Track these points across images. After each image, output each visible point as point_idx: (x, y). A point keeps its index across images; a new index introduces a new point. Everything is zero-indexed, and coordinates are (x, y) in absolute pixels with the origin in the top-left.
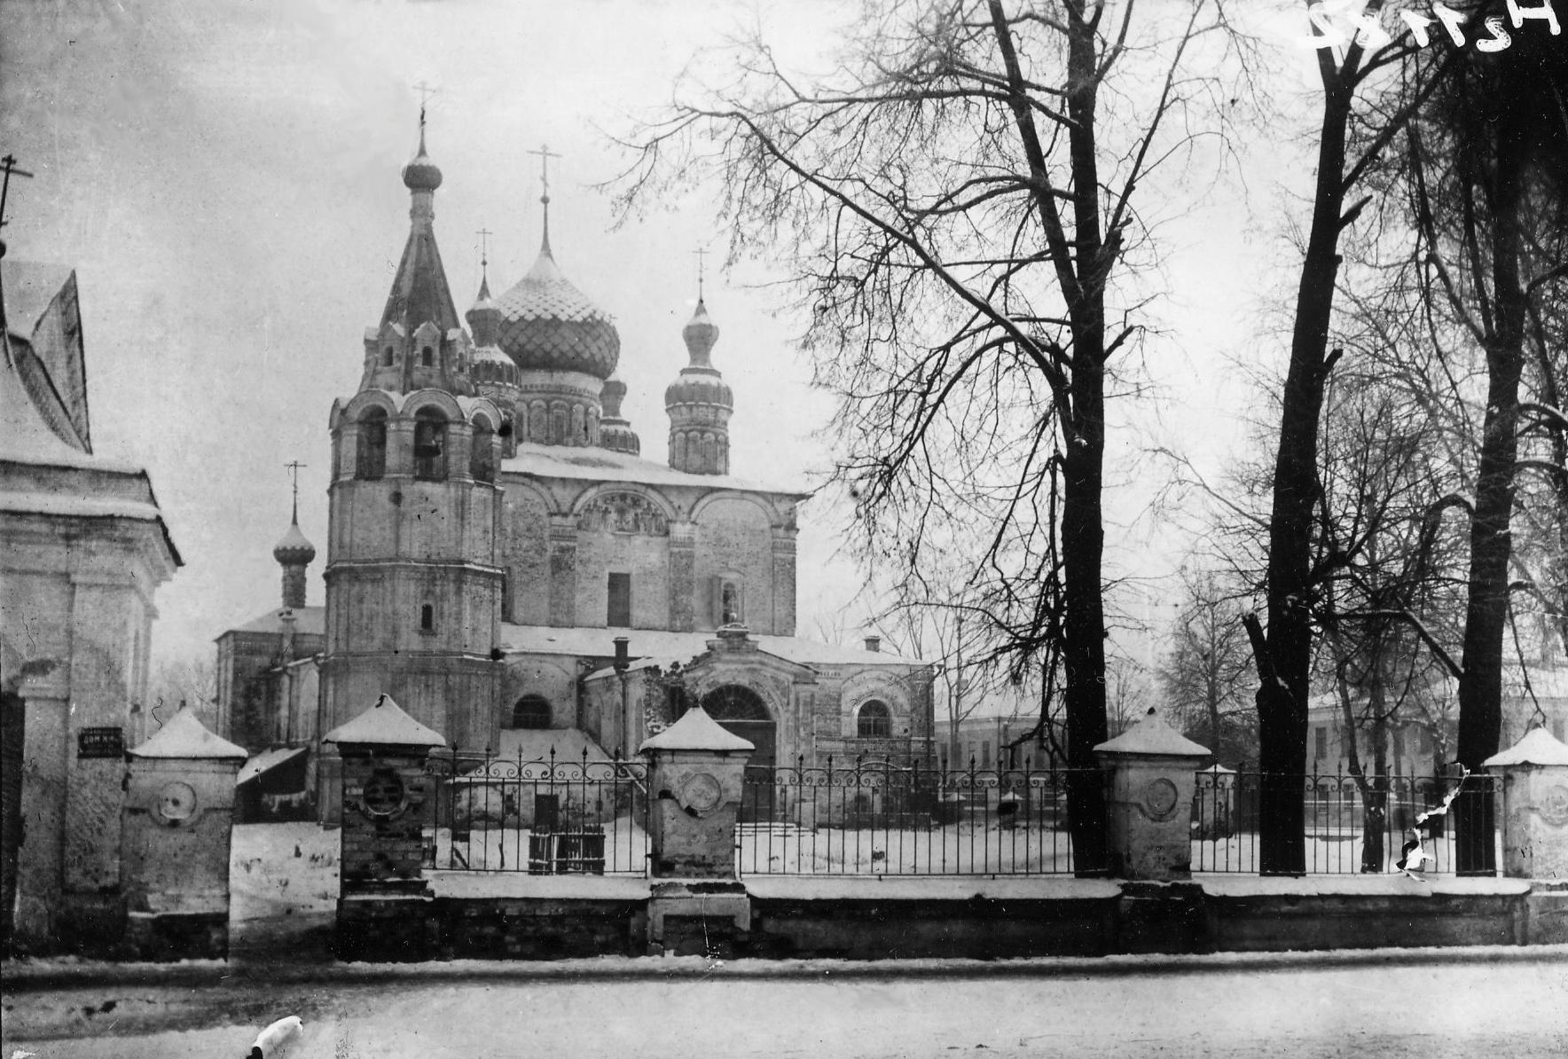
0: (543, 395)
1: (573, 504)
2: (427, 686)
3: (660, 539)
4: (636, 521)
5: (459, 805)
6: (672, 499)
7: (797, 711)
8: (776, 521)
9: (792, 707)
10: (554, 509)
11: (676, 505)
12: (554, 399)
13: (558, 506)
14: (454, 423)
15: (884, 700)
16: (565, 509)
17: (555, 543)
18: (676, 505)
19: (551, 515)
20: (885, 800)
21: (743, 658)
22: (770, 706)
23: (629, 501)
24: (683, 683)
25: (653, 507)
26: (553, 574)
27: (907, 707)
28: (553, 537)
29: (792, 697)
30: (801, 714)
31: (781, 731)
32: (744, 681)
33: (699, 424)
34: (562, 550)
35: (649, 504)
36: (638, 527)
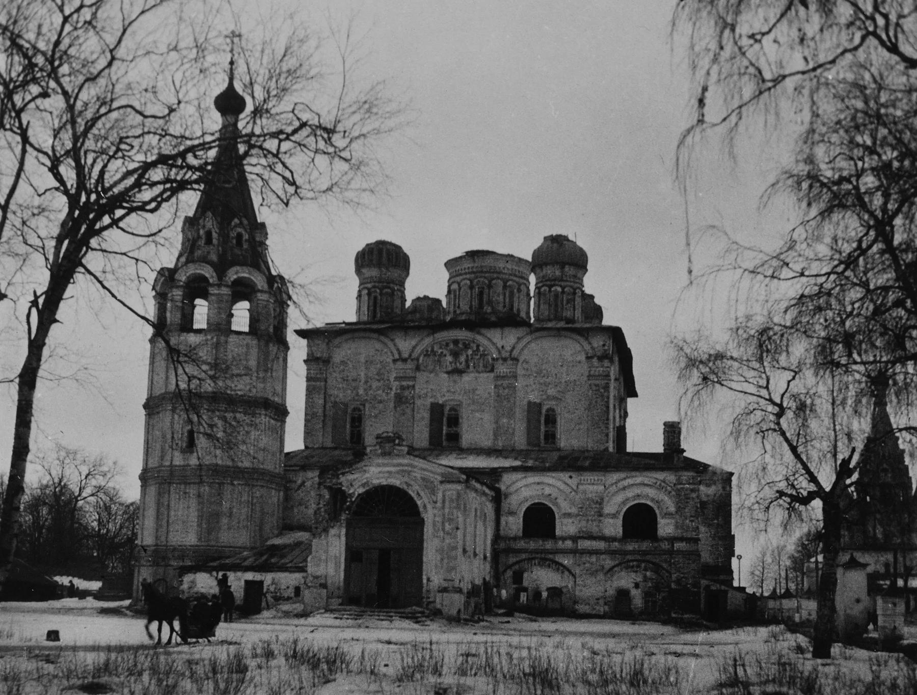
0: (468, 276)
1: (413, 351)
2: (185, 493)
3: (485, 375)
4: (467, 361)
5: (182, 587)
6: (495, 340)
7: (443, 508)
8: (591, 353)
9: (439, 505)
10: (397, 356)
11: (500, 346)
12: (554, 285)
13: (400, 353)
14: (262, 291)
15: (649, 503)
16: (406, 355)
17: (397, 383)
18: (500, 346)
19: (395, 361)
20: (647, 595)
21: (395, 461)
22: (419, 503)
23: (460, 346)
24: (341, 484)
25: (481, 349)
26: (395, 407)
27: (672, 509)
28: (396, 379)
29: (440, 495)
30: (447, 511)
31: (428, 530)
32: (396, 482)
33: (549, 280)
34: (403, 388)
35: (478, 346)
36: (468, 367)
